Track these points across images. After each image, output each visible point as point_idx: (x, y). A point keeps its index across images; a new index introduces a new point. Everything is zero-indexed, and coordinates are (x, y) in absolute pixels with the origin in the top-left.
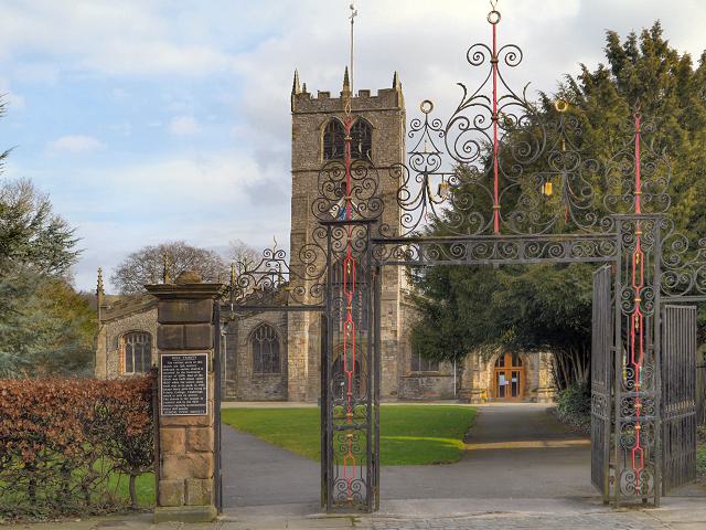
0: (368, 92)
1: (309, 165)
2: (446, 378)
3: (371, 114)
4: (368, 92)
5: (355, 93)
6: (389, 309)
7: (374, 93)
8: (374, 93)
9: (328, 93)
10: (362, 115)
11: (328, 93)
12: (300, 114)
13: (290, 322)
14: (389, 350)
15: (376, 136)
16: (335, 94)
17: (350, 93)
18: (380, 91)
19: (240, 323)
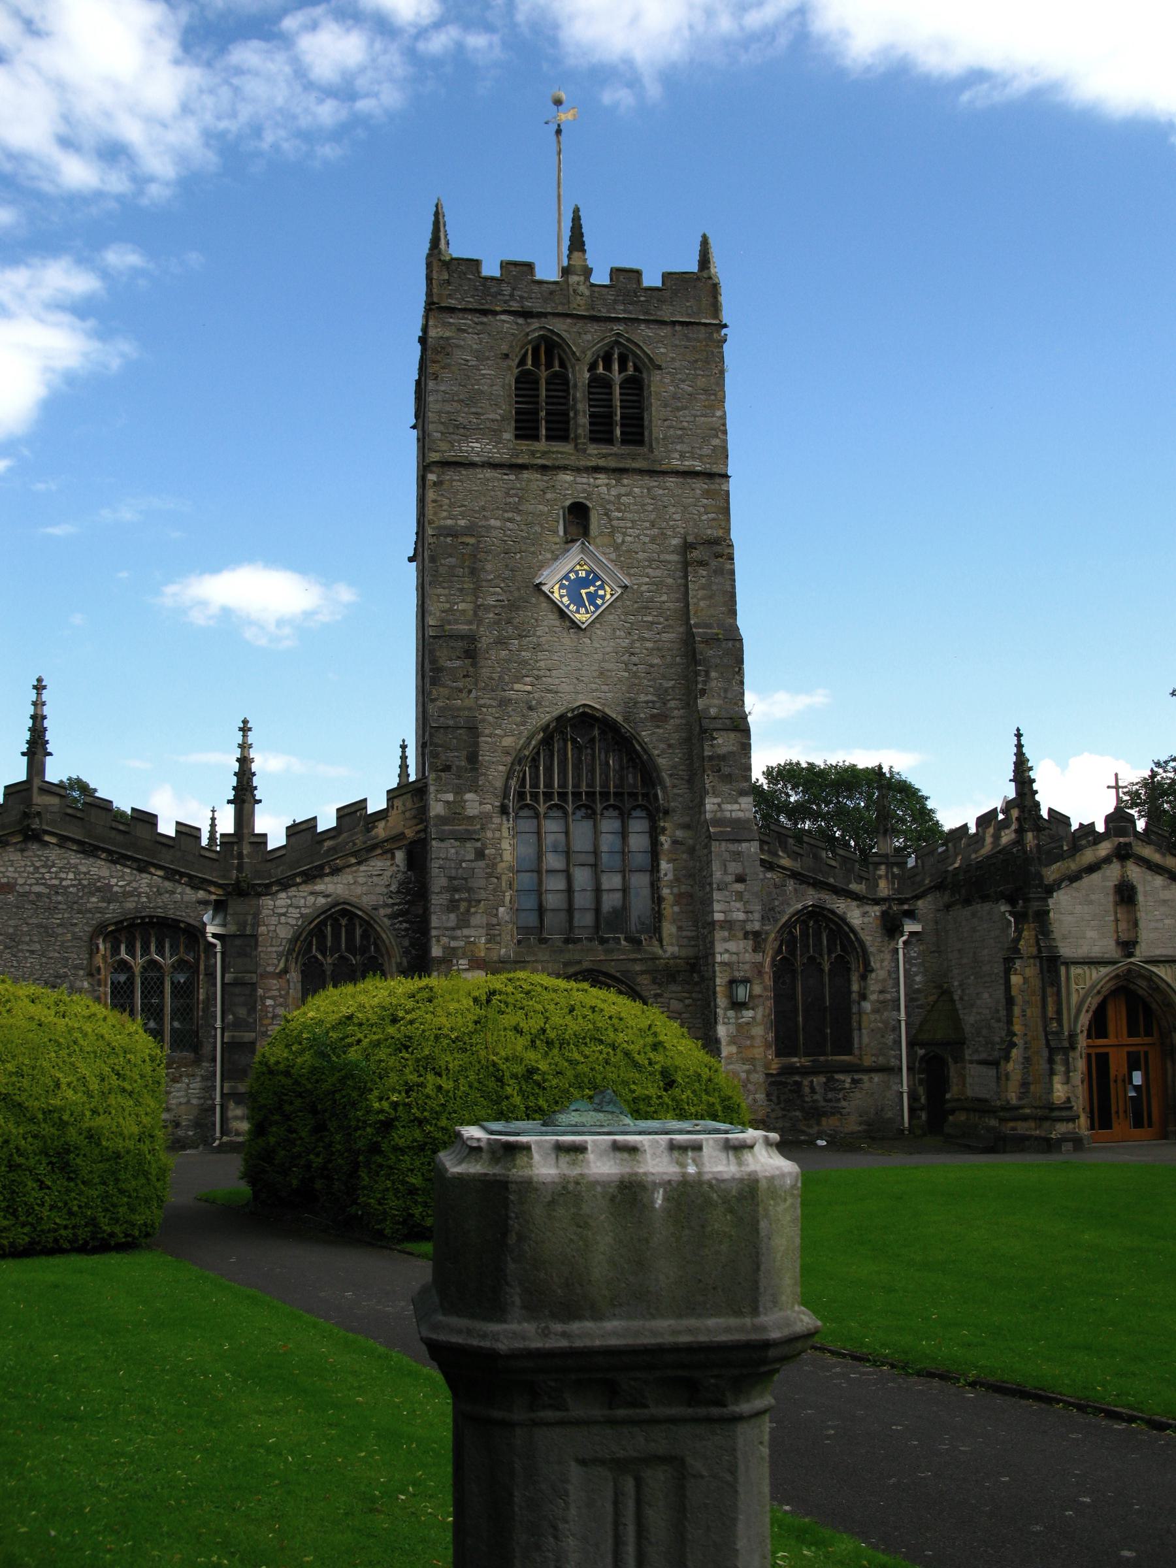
0: (638, 273)
1: (476, 448)
2: (877, 1078)
3: (645, 331)
4: (638, 273)
5: (601, 277)
6: (734, 868)
7: (652, 279)
8: (652, 279)
9: (529, 266)
10: (619, 328)
11: (529, 266)
12: (451, 310)
13: (438, 900)
14: (742, 993)
15: (660, 386)
16: (548, 271)
17: (588, 272)
18: (666, 276)
19: (267, 902)
